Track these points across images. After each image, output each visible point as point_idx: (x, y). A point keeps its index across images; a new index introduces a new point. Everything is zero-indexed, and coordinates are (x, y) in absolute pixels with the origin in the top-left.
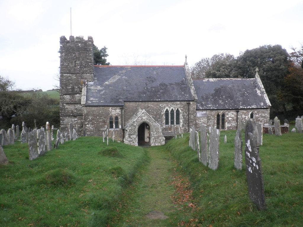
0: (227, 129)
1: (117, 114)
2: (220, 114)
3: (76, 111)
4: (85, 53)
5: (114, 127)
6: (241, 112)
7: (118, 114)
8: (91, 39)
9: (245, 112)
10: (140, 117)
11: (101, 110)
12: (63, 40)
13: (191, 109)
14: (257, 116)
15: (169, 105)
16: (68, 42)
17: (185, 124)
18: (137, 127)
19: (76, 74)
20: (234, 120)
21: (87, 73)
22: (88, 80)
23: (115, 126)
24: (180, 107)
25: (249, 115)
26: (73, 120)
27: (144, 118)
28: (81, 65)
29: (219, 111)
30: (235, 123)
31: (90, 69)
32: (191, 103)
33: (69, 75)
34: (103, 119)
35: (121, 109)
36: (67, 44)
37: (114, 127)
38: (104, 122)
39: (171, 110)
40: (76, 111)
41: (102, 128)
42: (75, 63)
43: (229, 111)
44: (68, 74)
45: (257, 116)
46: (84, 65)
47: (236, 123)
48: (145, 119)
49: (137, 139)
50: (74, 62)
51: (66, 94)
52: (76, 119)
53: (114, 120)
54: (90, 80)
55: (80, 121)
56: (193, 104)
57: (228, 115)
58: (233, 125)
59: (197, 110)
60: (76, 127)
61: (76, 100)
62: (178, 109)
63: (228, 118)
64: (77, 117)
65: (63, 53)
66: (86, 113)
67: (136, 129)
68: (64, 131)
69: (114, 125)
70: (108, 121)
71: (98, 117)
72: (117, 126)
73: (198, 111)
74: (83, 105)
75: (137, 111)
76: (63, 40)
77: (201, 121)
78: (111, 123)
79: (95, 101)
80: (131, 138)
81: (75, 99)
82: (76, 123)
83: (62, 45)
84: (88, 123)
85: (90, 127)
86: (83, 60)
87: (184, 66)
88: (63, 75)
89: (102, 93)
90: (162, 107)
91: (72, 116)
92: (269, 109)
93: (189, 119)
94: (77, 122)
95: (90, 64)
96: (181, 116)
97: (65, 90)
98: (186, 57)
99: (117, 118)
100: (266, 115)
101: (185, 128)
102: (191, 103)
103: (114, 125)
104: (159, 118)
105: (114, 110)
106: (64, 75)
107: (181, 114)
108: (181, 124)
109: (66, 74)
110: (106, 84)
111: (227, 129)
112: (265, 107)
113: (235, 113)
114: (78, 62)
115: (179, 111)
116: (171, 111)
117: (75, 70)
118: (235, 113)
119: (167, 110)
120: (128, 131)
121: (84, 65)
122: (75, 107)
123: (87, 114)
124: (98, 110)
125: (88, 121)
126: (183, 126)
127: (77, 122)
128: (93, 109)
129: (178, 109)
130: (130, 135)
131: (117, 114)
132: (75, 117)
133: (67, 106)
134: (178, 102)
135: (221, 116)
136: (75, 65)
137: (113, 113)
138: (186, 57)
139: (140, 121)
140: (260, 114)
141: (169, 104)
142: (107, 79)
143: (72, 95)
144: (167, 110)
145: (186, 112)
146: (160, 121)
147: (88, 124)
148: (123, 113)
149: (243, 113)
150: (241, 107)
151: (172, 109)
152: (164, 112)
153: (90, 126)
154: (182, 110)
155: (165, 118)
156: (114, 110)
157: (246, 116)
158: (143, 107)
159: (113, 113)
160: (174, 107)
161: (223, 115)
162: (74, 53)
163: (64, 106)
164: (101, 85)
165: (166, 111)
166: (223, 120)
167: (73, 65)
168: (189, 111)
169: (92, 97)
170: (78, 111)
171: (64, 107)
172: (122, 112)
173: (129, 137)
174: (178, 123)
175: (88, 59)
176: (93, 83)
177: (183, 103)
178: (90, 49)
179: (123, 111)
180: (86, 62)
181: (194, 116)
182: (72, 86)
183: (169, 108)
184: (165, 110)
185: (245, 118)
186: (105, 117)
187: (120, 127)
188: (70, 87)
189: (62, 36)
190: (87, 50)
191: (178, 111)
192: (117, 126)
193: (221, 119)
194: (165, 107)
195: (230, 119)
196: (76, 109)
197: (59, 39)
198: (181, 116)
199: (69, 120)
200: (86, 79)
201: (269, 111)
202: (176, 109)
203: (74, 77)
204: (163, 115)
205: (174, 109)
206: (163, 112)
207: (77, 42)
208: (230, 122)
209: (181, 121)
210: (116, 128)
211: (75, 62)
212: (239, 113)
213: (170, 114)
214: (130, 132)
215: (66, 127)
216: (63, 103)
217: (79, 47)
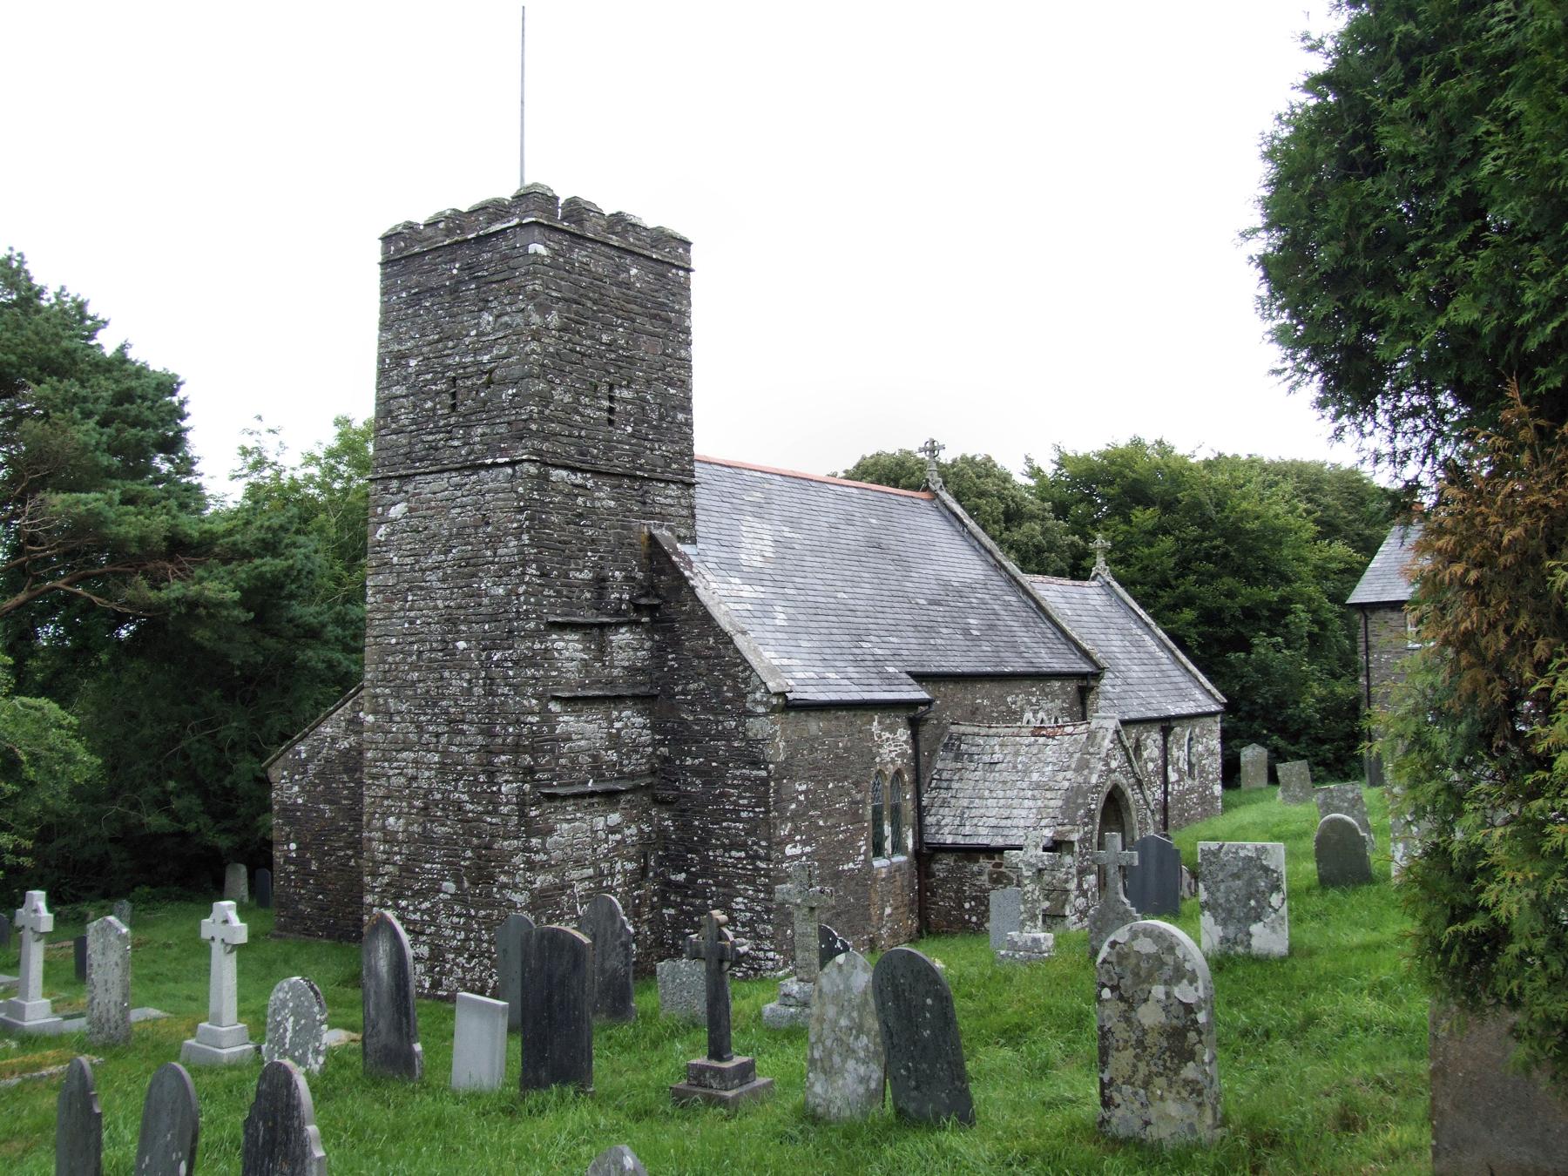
6: (1181, 732)
26: (600, 823)
33: (578, 479)
42: (611, 399)
44: (574, 470)
50: (604, 389)
51: (561, 627)
52: (615, 818)
60: (612, 875)
61: (615, 672)
64: (623, 798)
70: (869, 812)
82: (614, 849)
88: (545, 478)
91: (592, 794)
94: (618, 837)
97: (559, 594)
109: (564, 473)
127: (618, 837)
128: (814, 725)
132: (610, 797)
133: (567, 722)
134: (1057, 684)
143: (596, 631)
163: (548, 718)
167: (600, 409)
171: (553, 729)
180: (665, 396)
190: (668, 321)
196: (615, 741)
199: (575, 831)
211: (611, 388)
217: (628, 285)
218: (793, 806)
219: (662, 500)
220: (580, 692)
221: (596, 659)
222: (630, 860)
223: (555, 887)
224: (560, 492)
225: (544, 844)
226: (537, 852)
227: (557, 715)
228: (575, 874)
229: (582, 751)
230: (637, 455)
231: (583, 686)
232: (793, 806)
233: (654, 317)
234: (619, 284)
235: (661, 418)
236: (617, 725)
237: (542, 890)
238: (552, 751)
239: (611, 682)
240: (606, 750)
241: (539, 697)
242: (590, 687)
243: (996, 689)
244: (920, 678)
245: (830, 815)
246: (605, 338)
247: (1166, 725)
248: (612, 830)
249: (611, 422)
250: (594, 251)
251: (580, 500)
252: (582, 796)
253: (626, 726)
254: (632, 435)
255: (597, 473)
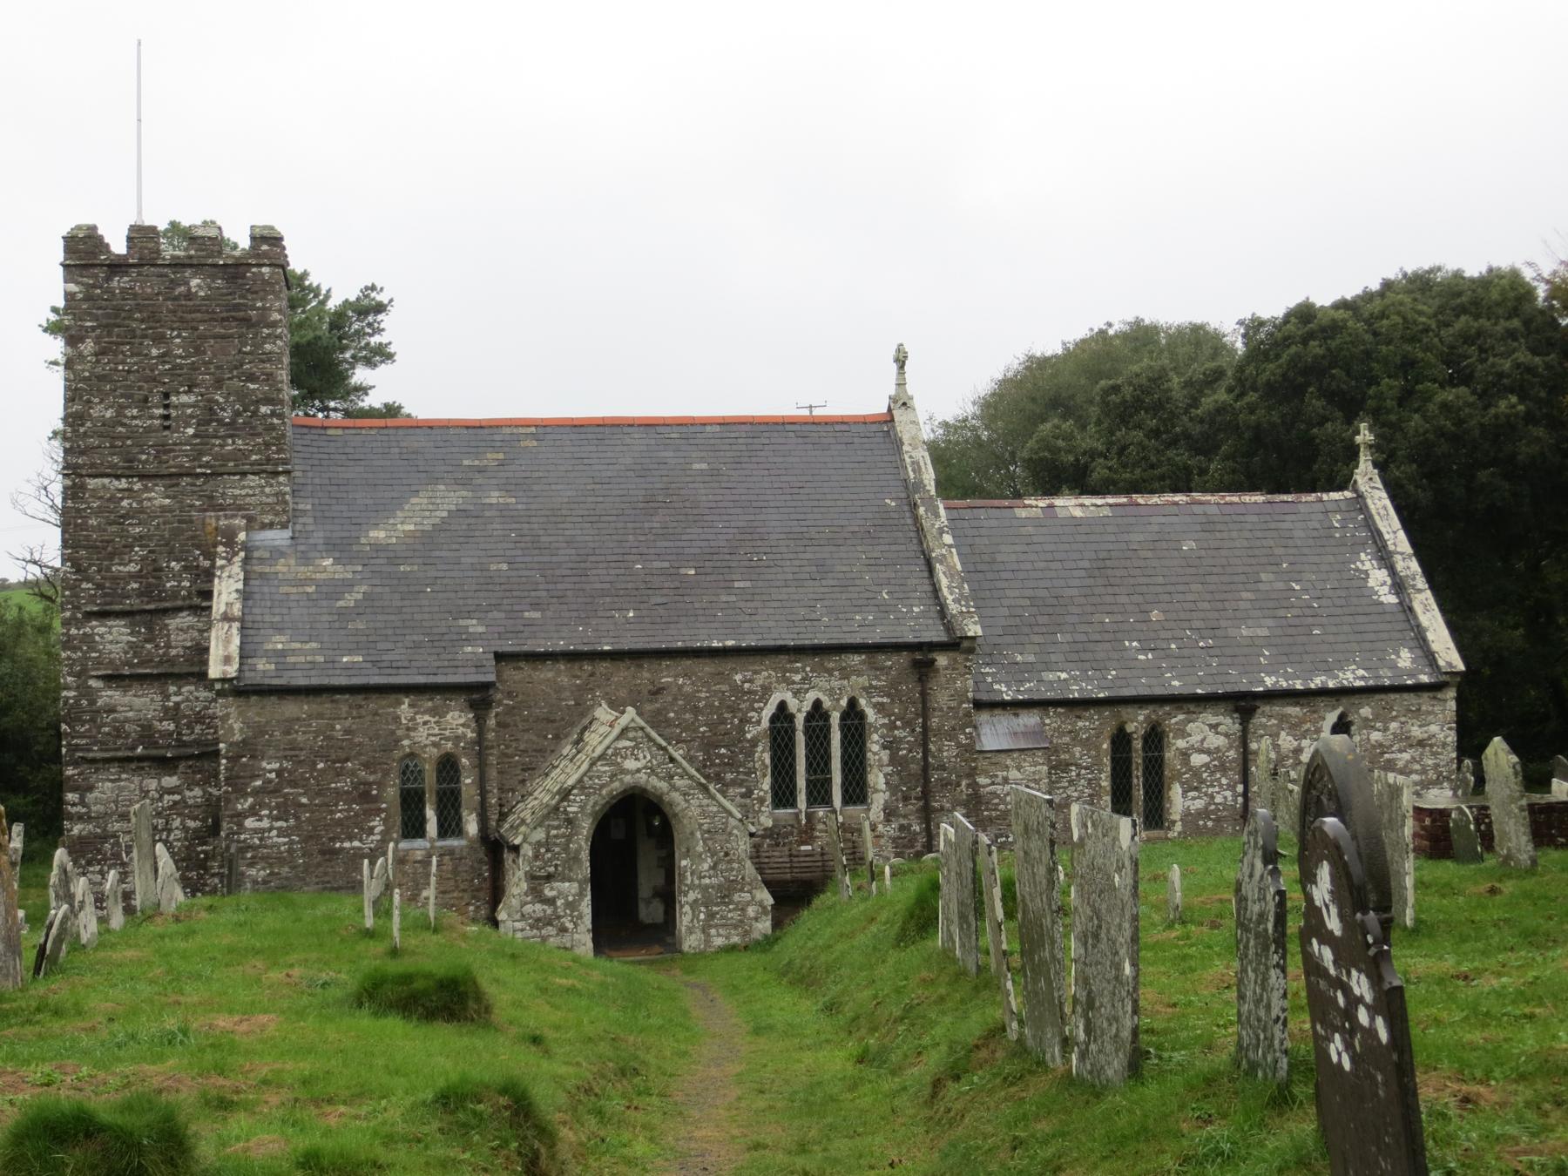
0: (1178, 827)
1: (447, 739)
2: (1130, 728)
3: (172, 727)
4: (231, 336)
5: (432, 827)
6: (1264, 718)
7: (457, 739)
8: (268, 242)
9: (1293, 711)
10: (602, 757)
11: (342, 720)
12: (83, 251)
13: (942, 698)
14: (1376, 736)
15: (797, 678)
16: (117, 266)
17: (906, 799)
18: (586, 827)
19: (171, 475)
20: (1223, 768)
21: (244, 474)
22: (250, 519)
23: (441, 825)
24: (868, 690)
25: (1318, 731)
26: (152, 784)
27: (630, 764)
28: (209, 412)
29: (1126, 712)
30: (1232, 787)
31: (267, 445)
32: (942, 660)
33: (123, 484)
34: (353, 773)
35: (473, 706)
36: (108, 279)
37: (432, 827)
38: (364, 795)
39: (807, 706)
40: (172, 727)
41: (351, 839)
42: (166, 407)
43: (1192, 707)
44: (118, 477)
45: (1376, 736)
46: (226, 415)
47: (1240, 788)
48: (638, 771)
49: (586, 907)
51: (103, 615)
52: (170, 781)
53: (430, 780)
54: (267, 519)
55: (197, 792)
56: (952, 666)
57: (1183, 734)
58: (1219, 799)
59: (979, 705)
60: (170, 831)
61: (173, 652)
62: (853, 703)
63: (1185, 755)
64: (182, 767)
65: (82, 340)
66: (238, 737)
67: (582, 843)
68: (89, 863)
69: (430, 814)
70: (392, 792)
71: (320, 766)
72: (450, 826)
73: (984, 717)
74: (218, 686)
75: (585, 721)
76: (83, 251)
77: (1006, 781)
78: (411, 803)
79: (302, 659)
80: (551, 902)
81: (168, 646)
82: (170, 808)
83: (77, 283)
84: (252, 807)
85: (270, 829)
86: (218, 383)
87: (889, 418)
88: (83, 487)
89: (349, 600)
90: (750, 692)
91: (140, 759)
92: (1451, 693)
93: (926, 768)
94: (177, 797)
95: (264, 409)
96: (875, 748)
97: (99, 586)
98: (901, 361)
99: (448, 766)
100: (1434, 728)
101: (902, 828)
102: (942, 660)
103: (430, 814)
104: (732, 764)
105: (427, 718)
106: (92, 483)
107: (875, 737)
108: (878, 800)
109: (106, 481)
110: (378, 547)
111: (1178, 827)
112: (1425, 679)
113: (1230, 723)
114: (184, 399)
115: (861, 716)
116: (810, 717)
117: (163, 449)
118: (1228, 721)
119: (782, 706)
120: (527, 851)
121: (226, 415)
122: (167, 697)
123: (249, 747)
124: (320, 716)
125: (256, 792)
126: (890, 813)
127: (177, 797)
129: (853, 703)
130: (537, 881)
131: (447, 739)
132: (164, 764)
133: (109, 696)
134: (856, 659)
135: (1138, 744)
136: (166, 417)
137: (421, 735)
138: (901, 361)
139: (602, 786)
140: (1394, 725)
141: (796, 671)
142: (383, 511)
144: (782, 706)
145: (908, 724)
146: (734, 783)
147: (253, 812)
148: (491, 735)
149: (1283, 718)
150: (1269, 681)
151: (817, 704)
152: (765, 723)
153: (265, 824)
154: (880, 708)
155: (768, 761)
156: (433, 712)
157: (1305, 743)
158: (623, 693)
159: (421, 735)
160: (830, 692)
161: (1155, 738)
162: (159, 339)
163: (90, 695)
164: (341, 549)
165: (773, 719)
166: (1155, 767)
167: (152, 417)
168: (925, 713)
169: (280, 630)
170: (190, 726)
171: (92, 702)
172: (481, 730)
173: (536, 893)
174: (856, 792)
175: (252, 378)
176: (287, 533)
177: (887, 661)
178: (264, 308)
179: (492, 722)
180: (242, 396)
181: (959, 745)
182: (143, 559)
183: (796, 694)
184: (769, 710)
185: (1298, 751)
186: (366, 766)
187: (472, 827)
188: (133, 568)
189: (79, 227)
190: (246, 321)
191: (852, 714)
192: (450, 826)
193: (1138, 759)
194: (767, 691)
195: (1198, 760)
196: (173, 713)
197: (61, 243)
198: (875, 748)
199: (121, 789)
200: (240, 508)
201: (1452, 705)
202: (844, 702)
203: (158, 497)
204: (754, 743)
205: (827, 703)
206: (759, 722)
207: (177, 265)
208: (1203, 781)
209: (877, 780)
210: (443, 832)
211: (167, 396)
212: (1259, 720)
213: (800, 738)
214: (536, 857)
215: (105, 837)
216: (82, 675)
217: (189, 296)
218: (259, 783)
219: (237, 492)
220: (126, 671)
221: (147, 641)
222: (195, 819)
223: (96, 836)
224: (101, 498)
225: (82, 799)
226: (74, 805)
227: (100, 690)
228: (117, 826)
229: (127, 720)
230: (201, 454)
231: (131, 665)
232: (259, 783)
233: (223, 320)
234: (176, 299)
235: (237, 414)
236: (175, 699)
237: (80, 837)
238: (93, 720)
239: (172, 661)
240: (161, 721)
241: (78, 675)
242: (141, 664)
243: (707, 667)
244: (500, 657)
245: (319, 794)
246: (154, 352)
247: (1244, 704)
248: (171, 791)
249: (167, 428)
250: (139, 274)
251: (125, 503)
252: (129, 760)
253: (187, 700)
254: (195, 436)
255: (142, 477)
